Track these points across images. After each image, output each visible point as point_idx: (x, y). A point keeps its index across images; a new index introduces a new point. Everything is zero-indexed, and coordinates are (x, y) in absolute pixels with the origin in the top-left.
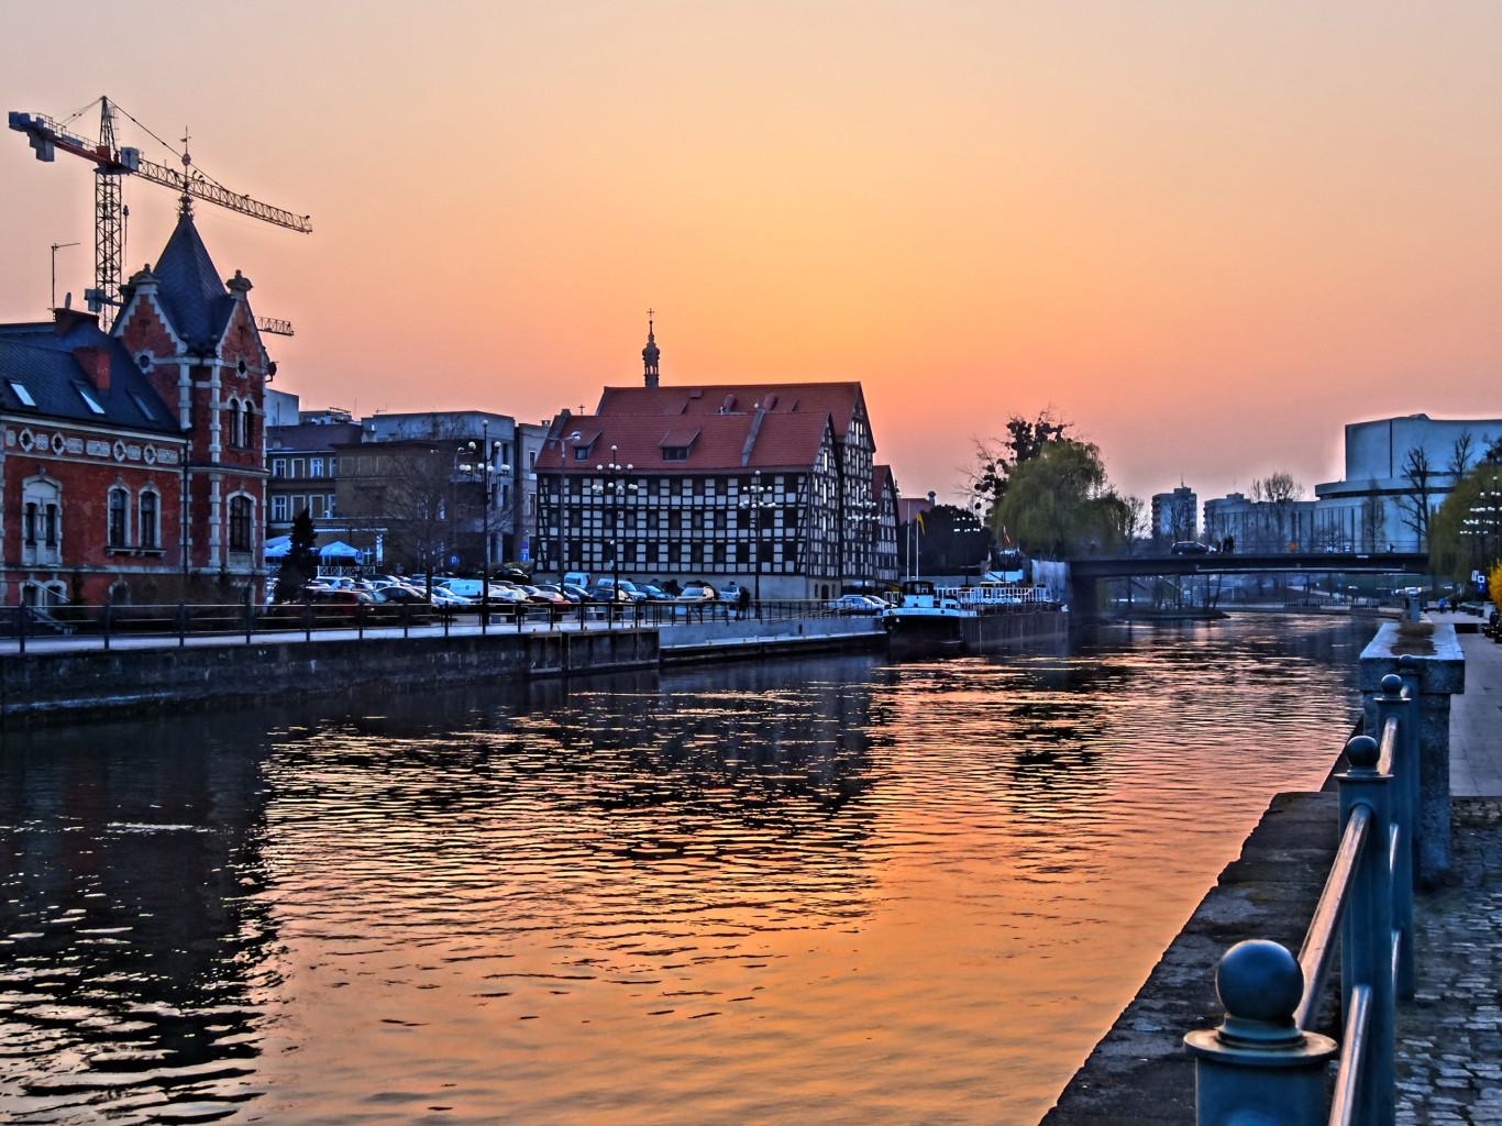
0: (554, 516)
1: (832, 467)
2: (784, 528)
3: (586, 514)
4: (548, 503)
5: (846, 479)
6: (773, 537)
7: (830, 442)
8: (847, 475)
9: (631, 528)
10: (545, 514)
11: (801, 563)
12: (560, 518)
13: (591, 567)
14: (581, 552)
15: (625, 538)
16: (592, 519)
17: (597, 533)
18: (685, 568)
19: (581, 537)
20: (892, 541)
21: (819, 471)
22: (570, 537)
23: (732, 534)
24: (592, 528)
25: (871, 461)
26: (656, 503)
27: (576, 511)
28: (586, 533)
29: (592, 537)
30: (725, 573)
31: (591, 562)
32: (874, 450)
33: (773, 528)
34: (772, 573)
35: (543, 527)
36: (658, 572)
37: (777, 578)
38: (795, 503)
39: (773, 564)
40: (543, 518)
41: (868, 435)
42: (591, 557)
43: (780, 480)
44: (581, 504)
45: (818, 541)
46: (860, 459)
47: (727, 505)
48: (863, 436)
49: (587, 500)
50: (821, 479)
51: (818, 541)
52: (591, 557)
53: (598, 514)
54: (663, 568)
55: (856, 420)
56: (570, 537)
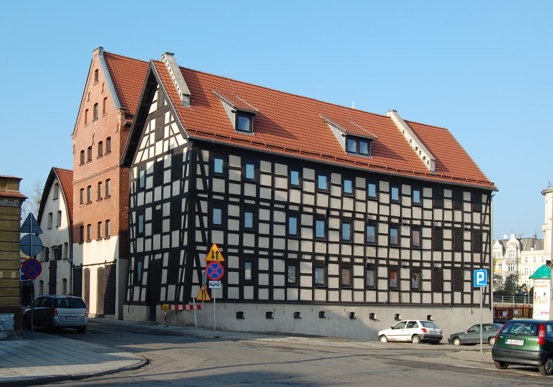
0: (217, 214)
2: (472, 252)
3: (264, 214)
4: (208, 190)
6: (462, 263)
9: (320, 240)
10: (204, 209)
12: (225, 217)
13: (271, 294)
14: (256, 272)
15: (314, 254)
16: (271, 223)
17: (279, 244)
18: (383, 297)
19: (256, 248)
22: (241, 247)
23: (427, 256)
24: (271, 236)
26: (326, 205)
27: (250, 206)
28: (264, 243)
29: (271, 249)
30: (421, 305)
31: (271, 287)
33: (462, 251)
34: (463, 305)
35: (202, 228)
36: (353, 303)
37: (469, 310)
39: (463, 293)
40: (201, 215)
42: (271, 280)
43: (467, 196)
44: (257, 199)
47: (422, 220)
49: (265, 194)
52: (271, 280)
53: (280, 217)
54: (359, 296)
56: (241, 247)
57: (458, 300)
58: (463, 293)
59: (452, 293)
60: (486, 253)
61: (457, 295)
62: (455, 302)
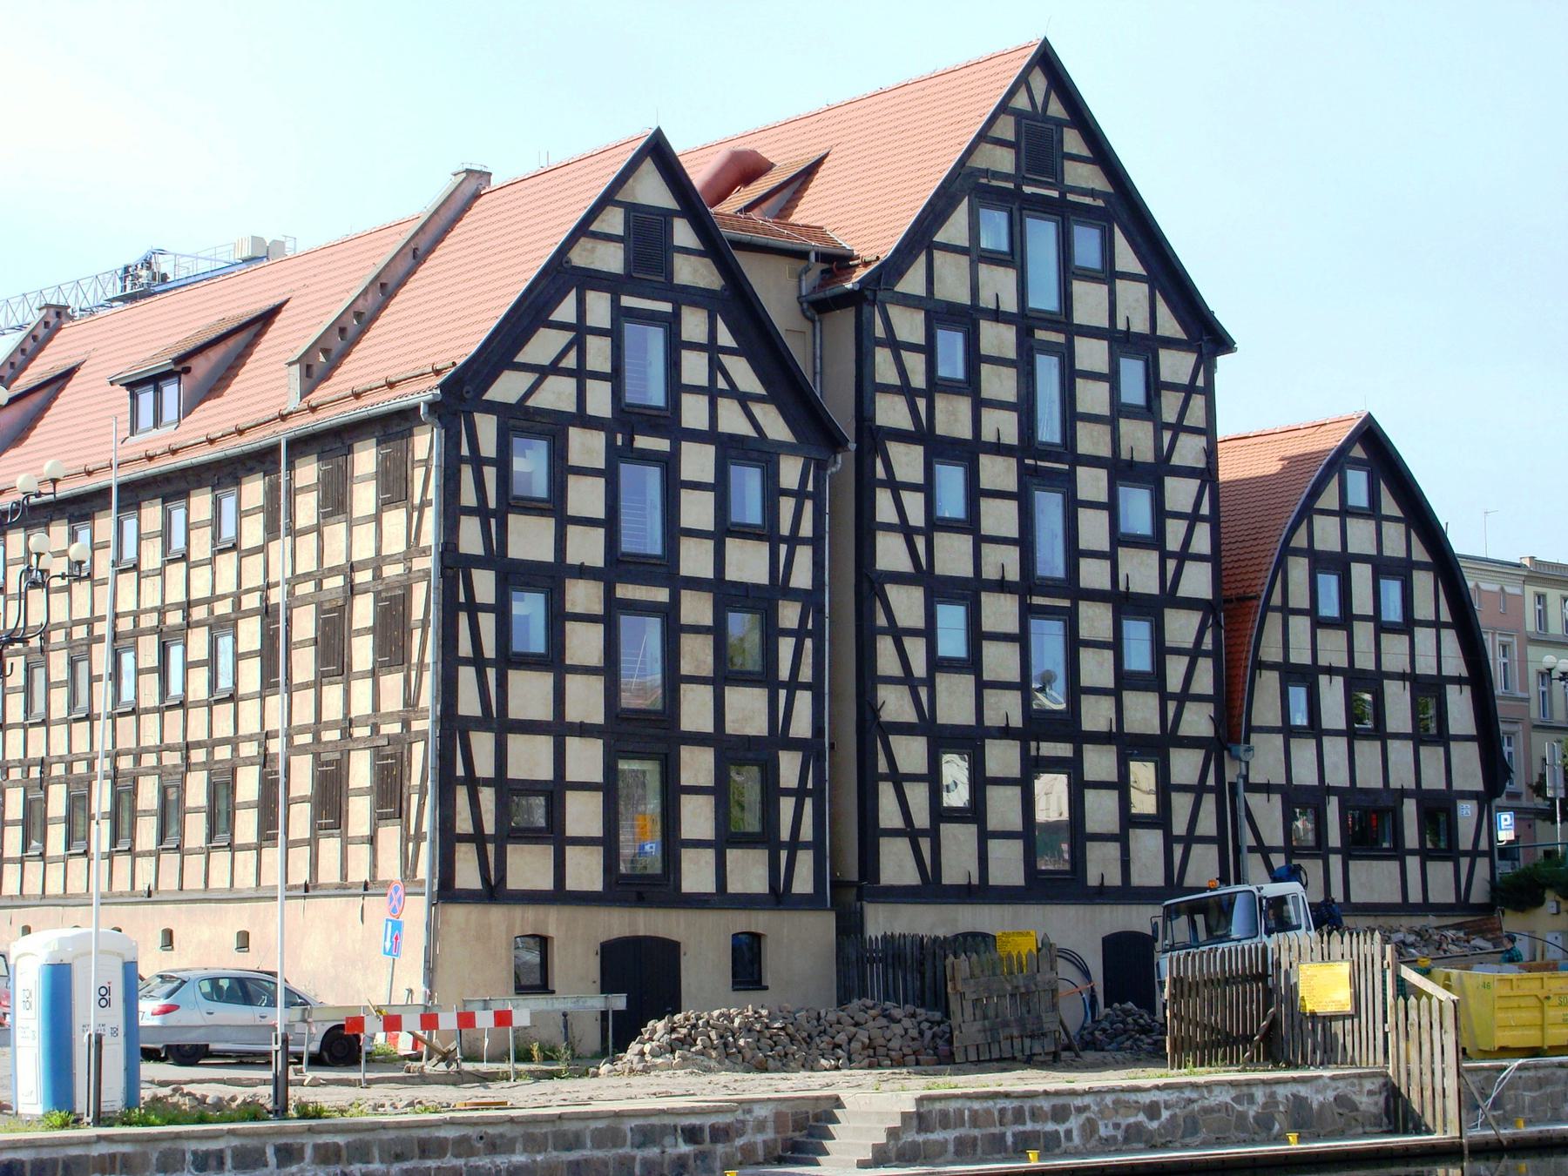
1: (712, 393)
5: (907, 461)
6: (348, 723)
7: (692, 271)
8: (923, 435)
11: (419, 837)
20: (1430, 731)
21: (557, 394)
25: (1202, 388)
32: (1209, 339)
34: (343, 888)
38: (406, 557)
39: (346, 842)
41: (1167, 275)
45: (559, 729)
46: (1069, 376)
48: (1108, 275)
50: (587, 447)
51: (559, 729)
55: (1018, 206)
57: (329, 873)
58: (346, 842)
59: (313, 843)
60: (421, 665)
61: (330, 847)
62: (323, 878)
